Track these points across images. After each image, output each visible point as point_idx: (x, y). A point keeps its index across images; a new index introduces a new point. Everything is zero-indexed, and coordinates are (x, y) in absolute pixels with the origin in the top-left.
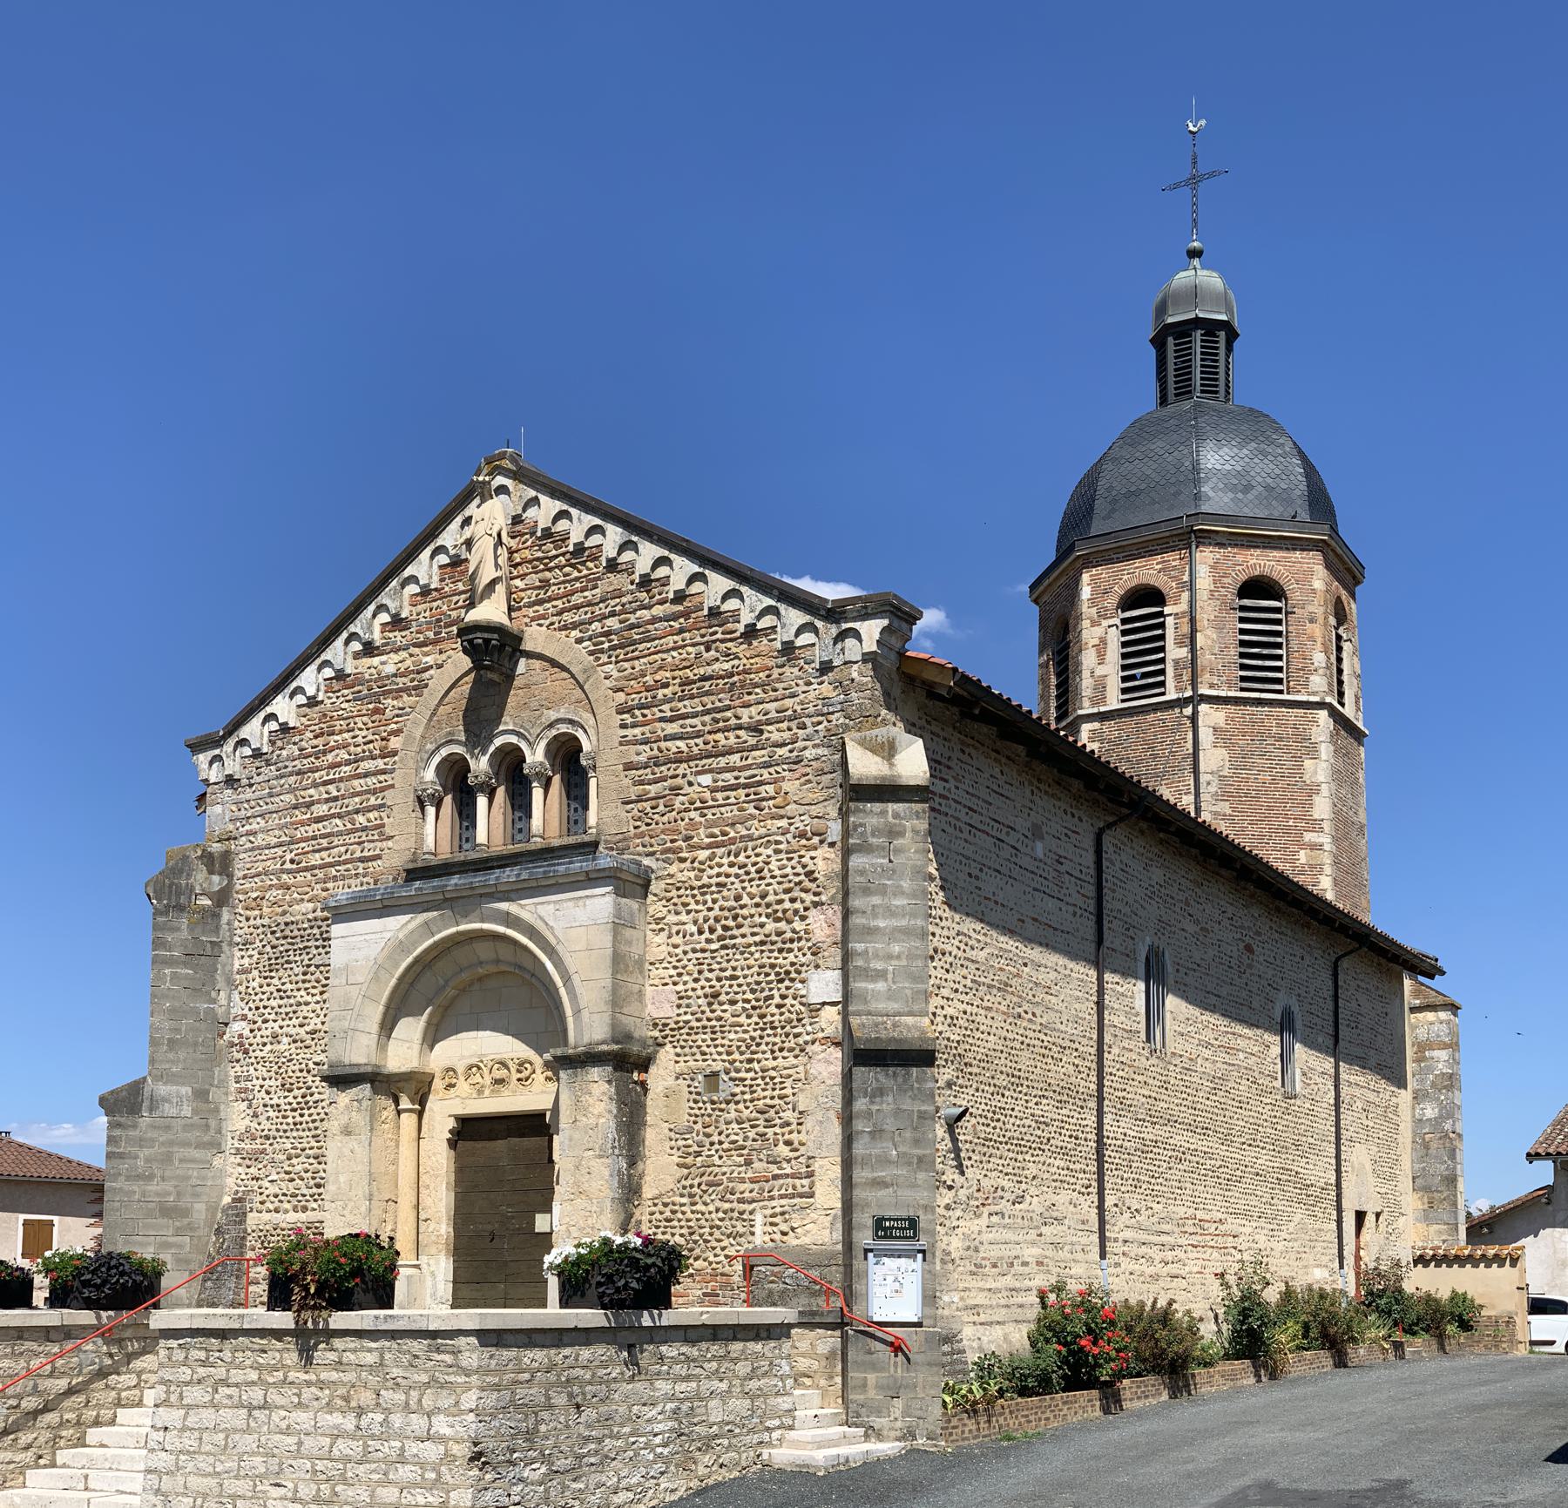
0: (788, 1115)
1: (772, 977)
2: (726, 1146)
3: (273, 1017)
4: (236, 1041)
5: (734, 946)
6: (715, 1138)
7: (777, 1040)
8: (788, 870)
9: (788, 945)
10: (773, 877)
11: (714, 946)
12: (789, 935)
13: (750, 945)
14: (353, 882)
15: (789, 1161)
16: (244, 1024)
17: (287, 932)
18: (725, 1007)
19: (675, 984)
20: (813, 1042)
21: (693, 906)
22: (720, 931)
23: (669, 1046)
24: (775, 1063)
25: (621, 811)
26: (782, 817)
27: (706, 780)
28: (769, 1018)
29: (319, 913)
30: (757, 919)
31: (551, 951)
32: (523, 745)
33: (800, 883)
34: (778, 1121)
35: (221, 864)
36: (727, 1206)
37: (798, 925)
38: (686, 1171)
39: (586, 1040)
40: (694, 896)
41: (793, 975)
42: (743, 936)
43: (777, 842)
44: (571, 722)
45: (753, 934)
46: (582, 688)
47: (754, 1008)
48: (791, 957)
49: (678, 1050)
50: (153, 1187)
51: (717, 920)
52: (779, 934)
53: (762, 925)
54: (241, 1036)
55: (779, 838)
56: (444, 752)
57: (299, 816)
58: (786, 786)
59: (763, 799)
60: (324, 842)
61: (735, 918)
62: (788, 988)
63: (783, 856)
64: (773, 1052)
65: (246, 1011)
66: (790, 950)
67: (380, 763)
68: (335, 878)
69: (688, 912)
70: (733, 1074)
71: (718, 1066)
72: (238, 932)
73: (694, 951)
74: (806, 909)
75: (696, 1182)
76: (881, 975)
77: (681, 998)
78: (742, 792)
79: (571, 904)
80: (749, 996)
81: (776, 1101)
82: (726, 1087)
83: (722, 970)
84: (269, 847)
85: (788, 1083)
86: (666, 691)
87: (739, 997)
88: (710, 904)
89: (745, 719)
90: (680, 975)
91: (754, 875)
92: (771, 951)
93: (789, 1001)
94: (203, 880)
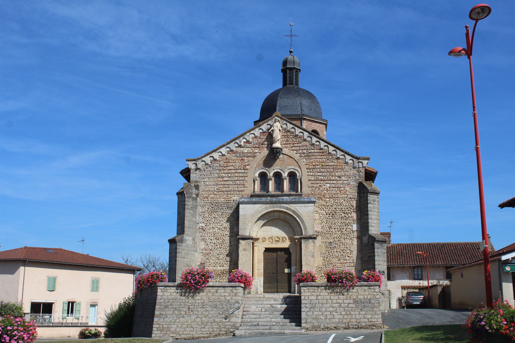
0: (348, 251)
25: (308, 189)
27: (328, 185)
31: (299, 216)
32: (282, 172)
35: (197, 187)
37: (350, 215)
39: (308, 234)
46: (297, 163)
50: (185, 260)
56: (261, 171)
57: (219, 179)
58: (347, 189)
60: (227, 186)
67: (243, 171)
68: (230, 194)
71: (332, 241)
76: (373, 226)
78: (336, 189)
82: (333, 245)
84: (210, 185)
89: (337, 175)
94: (194, 191)
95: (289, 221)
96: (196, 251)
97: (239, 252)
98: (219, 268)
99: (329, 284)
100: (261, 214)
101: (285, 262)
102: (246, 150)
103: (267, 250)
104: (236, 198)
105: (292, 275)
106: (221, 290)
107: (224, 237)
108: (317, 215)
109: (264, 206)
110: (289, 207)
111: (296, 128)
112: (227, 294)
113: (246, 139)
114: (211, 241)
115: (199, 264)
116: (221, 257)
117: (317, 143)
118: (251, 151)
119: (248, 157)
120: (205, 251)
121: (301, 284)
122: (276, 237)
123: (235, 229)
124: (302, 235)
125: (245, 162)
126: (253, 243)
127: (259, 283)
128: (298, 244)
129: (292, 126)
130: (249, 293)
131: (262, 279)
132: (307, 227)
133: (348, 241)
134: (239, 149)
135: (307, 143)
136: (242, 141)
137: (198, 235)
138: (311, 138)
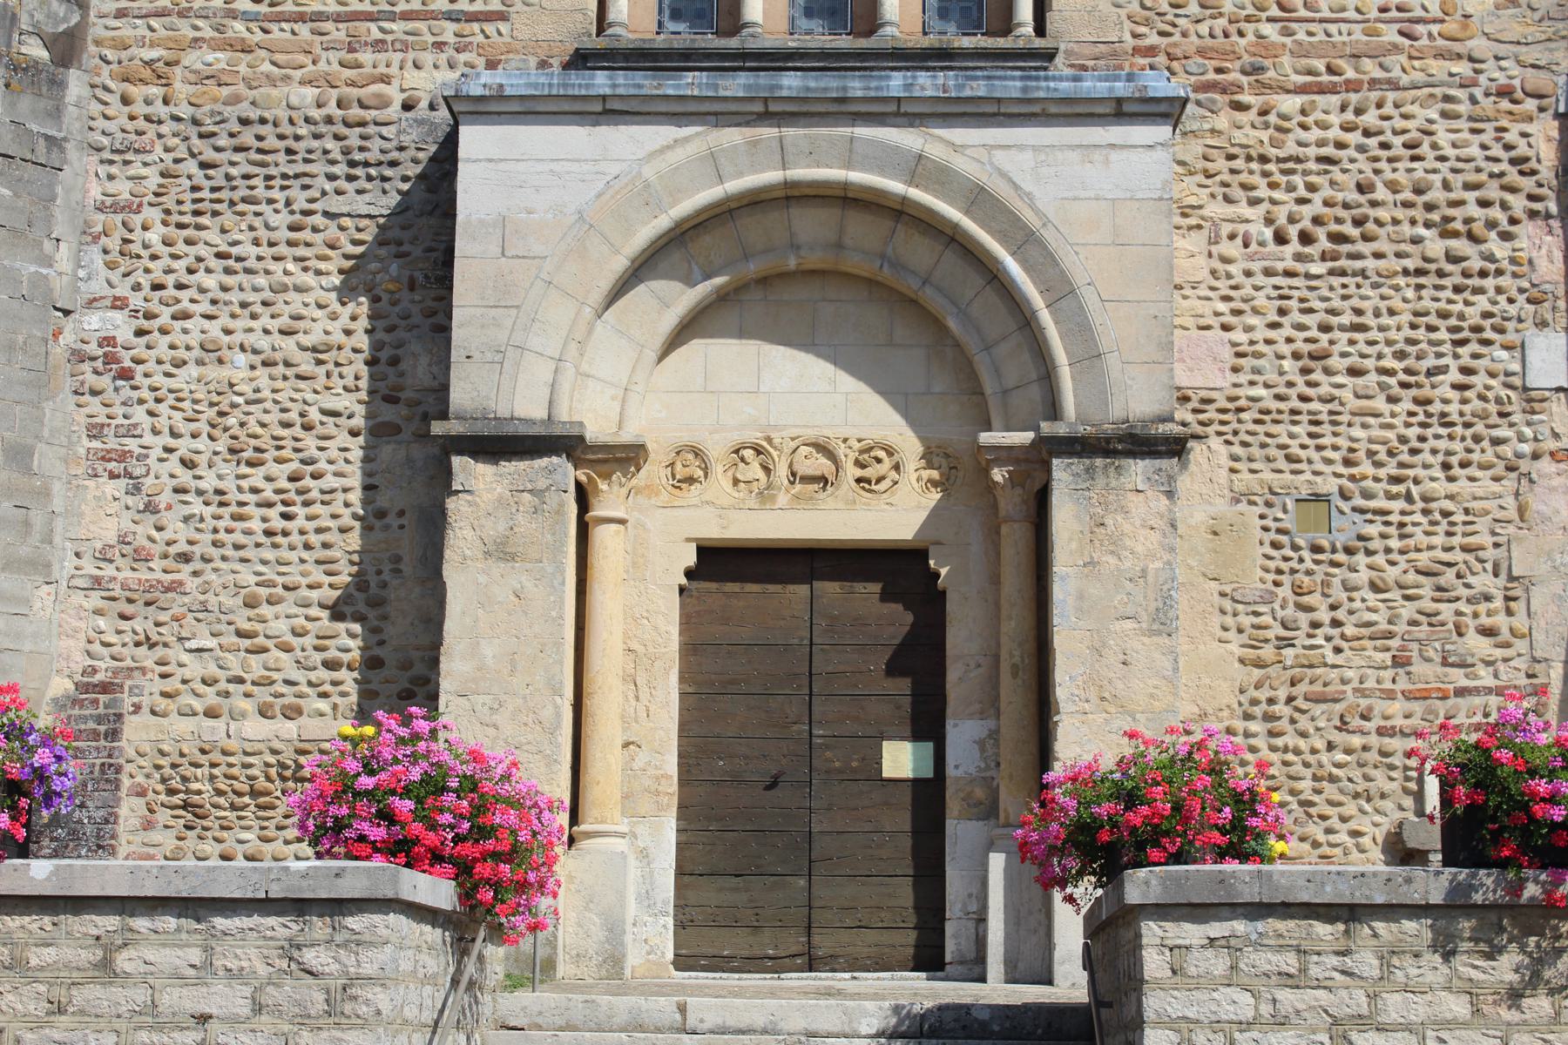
0: (1482, 581)
1: (1443, 335)
2: (1349, 630)
3: (205, 307)
4: (93, 349)
5: (1363, 273)
6: (1324, 616)
7: (1457, 446)
8: (1474, 151)
9: (1476, 282)
10: (1443, 159)
11: (1317, 268)
12: (1476, 264)
13: (1396, 274)
14: (428, 58)
15: (1488, 663)
16: (118, 316)
17: (247, 138)
18: (1339, 379)
19: (1226, 328)
20: (1536, 456)
21: (1263, 192)
22: (1324, 243)
23: (1215, 443)
24: (1453, 488)
26: (1459, 56)
28: (1436, 408)
29: (332, 109)
30: (1407, 230)
31: (1025, 240)
33: (1502, 174)
34: (1465, 592)
36: (1356, 741)
37: (1500, 250)
38: (1257, 673)
39: (1117, 411)
40: (1265, 174)
41: (1489, 334)
42: (1378, 256)
43: (1447, 99)
45: (1398, 255)
47: (1404, 385)
48: (1482, 302)
49: (1237, 450)
51: (1317, 221)
52: (1453, 259)
53: (1416, 241)
54: (109, 341)
55: (1452, 92)
59: (1418, 21)
61: (1358, 223)
62: (1475, 356)
63: (1463, 124)
64: (1446, 466)
65: (123, 290)
66: (1479, 291)
68: (379, 45)
69: (1254, 202)
70: (1359, 502)
71: (1329, 485)
72: (100, 123)
73: (1268, 273)
74: (1513, 221)
75: (1282, 694)
77: (1239, 355)
79: (1073, 156)
80: (1389, 363)
81: (1457, 556)
83: (1332, 312)
85: (1482, 524)
87: (1369, 363)
88: (1302, 192)
90: (1237, 313)
91: (1398, 150)
92: (1437, 288)
93: (1479, 380)
95: (930, 297)
96: (41, 568)
97: (454, 576)
98: (256, 728)
99: (1487, 885)
100: (663, 222)
101: (893, 669)
103: (718, 563)
104: (431, 80)
105: (953, 805)
106: (161, 947)
107: (310, 443)
108: (1196, 242)
109: (695, 140)
110: (935, 151)
112: (235, 1000)
114: (185, 477)
115: (62, 686)
116: (281, 627)
120: (122, 573)
121: (1141, 884)
122: (811, 437)
123: (419, 371)
124: (1054, 410)
126: (583, 497)
127: (634, 870)
128: (1011, 504)
130: (537, 972)
131: (663, 837)
132: (1105, 344)
133: (1486, 485)
137: (65, 414)
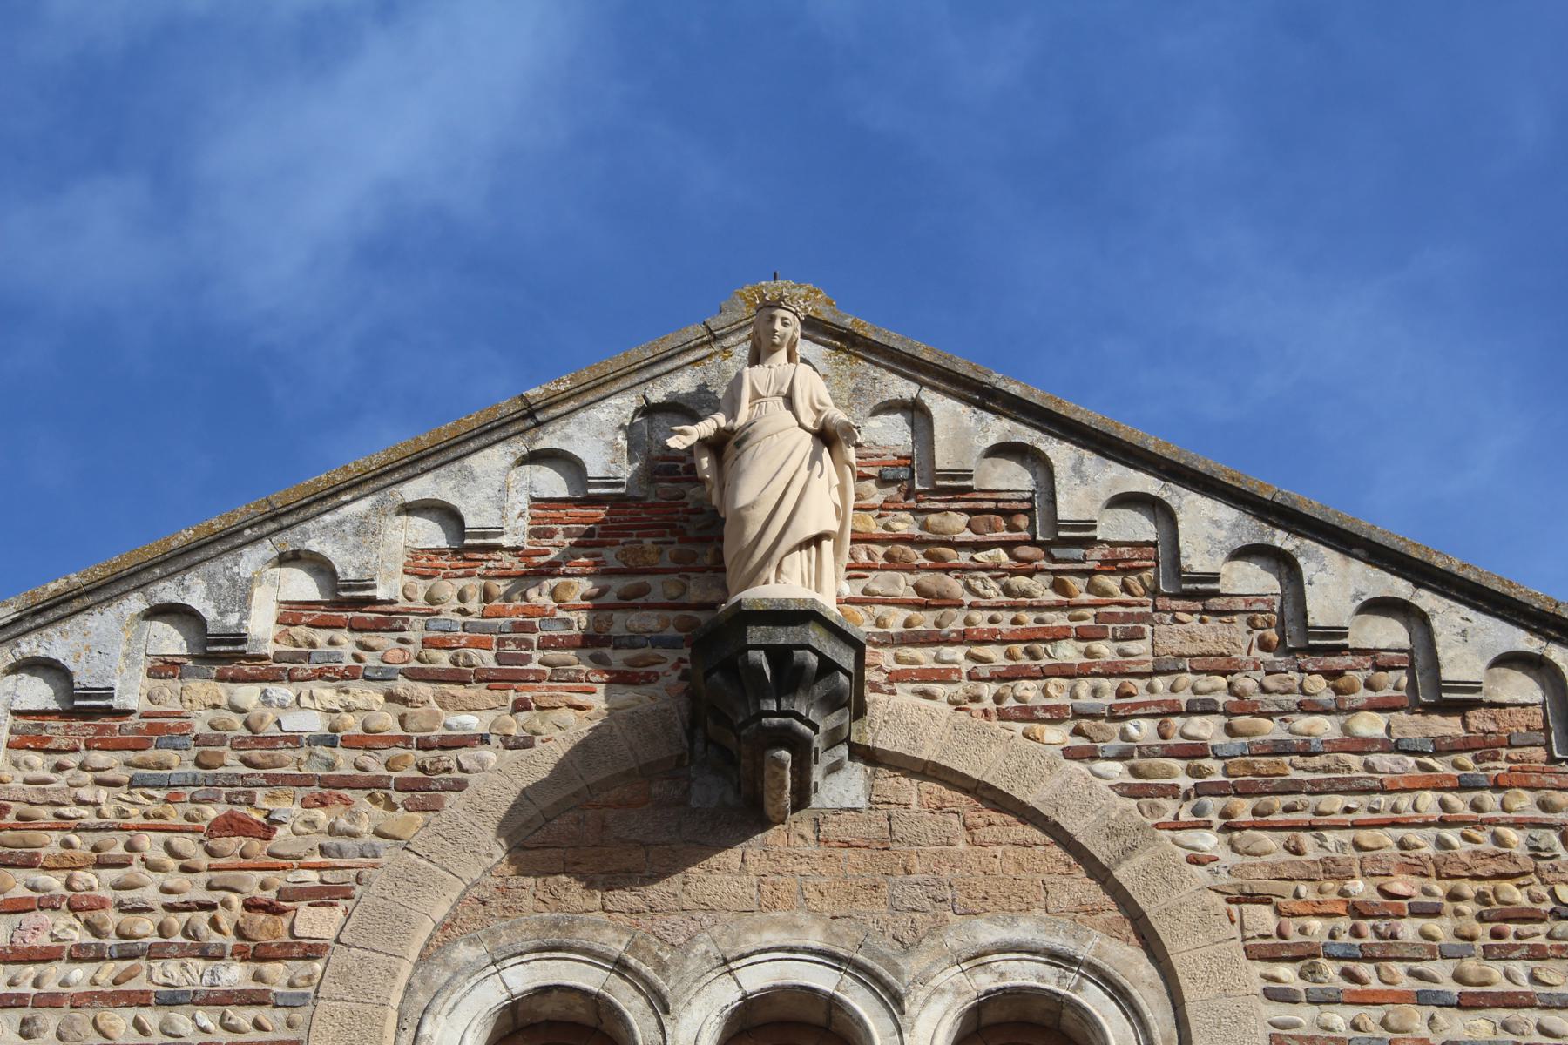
32: (861, 1002)
44: (1058, 958)
46: (1100, 873)
56: (522, 978)
67: (235, 975)
86: (1432, 925)
102: (304, 710)
111: (1060, 453)
113: (319, 566)
117: (1390, 634)
118: (387, 720)
119: (330, 788)
125: (278, 862)
129: (999, 429)
134: (201, 701)
135: (1236, 638)
136: (264, 597)
138: (1285, 565)
